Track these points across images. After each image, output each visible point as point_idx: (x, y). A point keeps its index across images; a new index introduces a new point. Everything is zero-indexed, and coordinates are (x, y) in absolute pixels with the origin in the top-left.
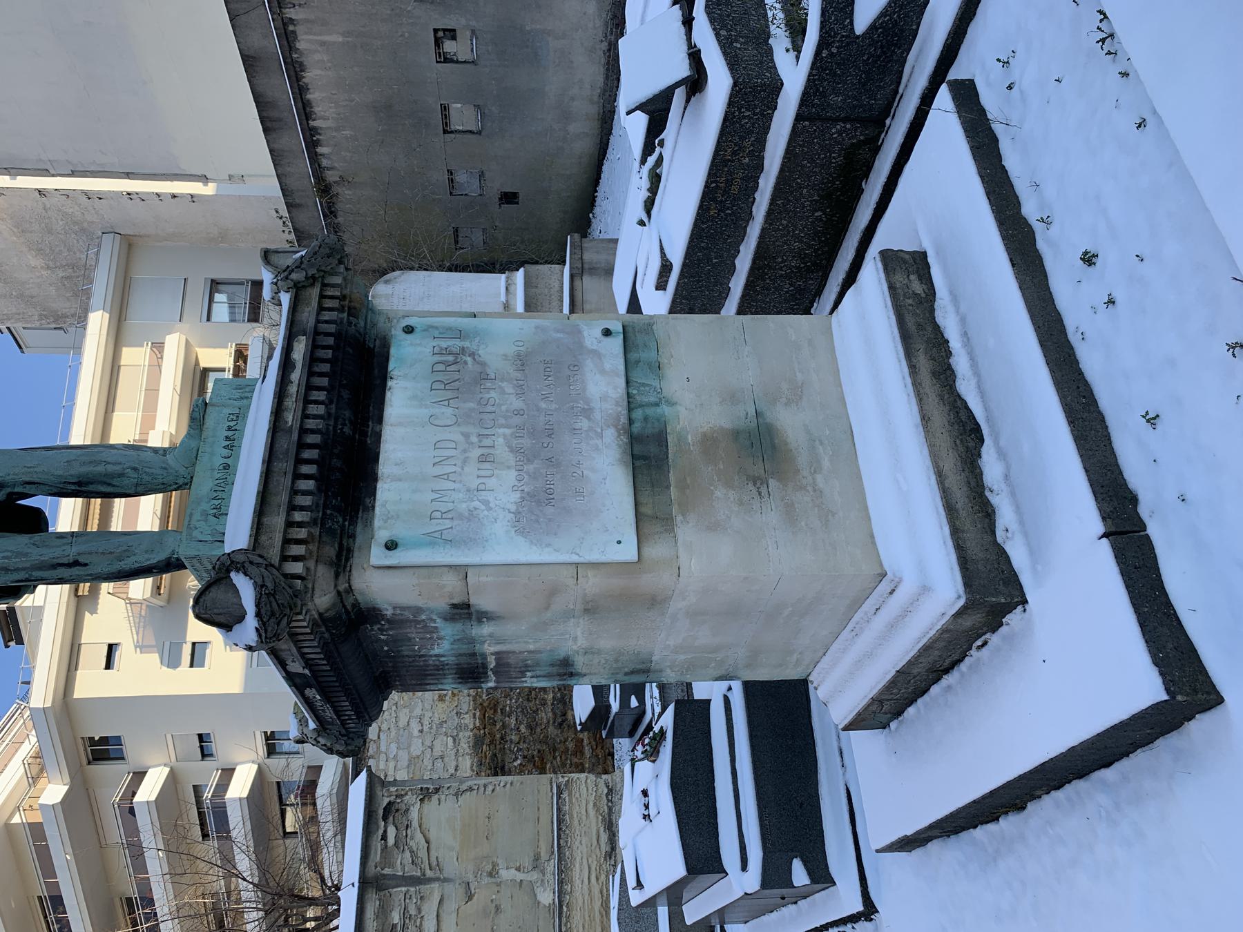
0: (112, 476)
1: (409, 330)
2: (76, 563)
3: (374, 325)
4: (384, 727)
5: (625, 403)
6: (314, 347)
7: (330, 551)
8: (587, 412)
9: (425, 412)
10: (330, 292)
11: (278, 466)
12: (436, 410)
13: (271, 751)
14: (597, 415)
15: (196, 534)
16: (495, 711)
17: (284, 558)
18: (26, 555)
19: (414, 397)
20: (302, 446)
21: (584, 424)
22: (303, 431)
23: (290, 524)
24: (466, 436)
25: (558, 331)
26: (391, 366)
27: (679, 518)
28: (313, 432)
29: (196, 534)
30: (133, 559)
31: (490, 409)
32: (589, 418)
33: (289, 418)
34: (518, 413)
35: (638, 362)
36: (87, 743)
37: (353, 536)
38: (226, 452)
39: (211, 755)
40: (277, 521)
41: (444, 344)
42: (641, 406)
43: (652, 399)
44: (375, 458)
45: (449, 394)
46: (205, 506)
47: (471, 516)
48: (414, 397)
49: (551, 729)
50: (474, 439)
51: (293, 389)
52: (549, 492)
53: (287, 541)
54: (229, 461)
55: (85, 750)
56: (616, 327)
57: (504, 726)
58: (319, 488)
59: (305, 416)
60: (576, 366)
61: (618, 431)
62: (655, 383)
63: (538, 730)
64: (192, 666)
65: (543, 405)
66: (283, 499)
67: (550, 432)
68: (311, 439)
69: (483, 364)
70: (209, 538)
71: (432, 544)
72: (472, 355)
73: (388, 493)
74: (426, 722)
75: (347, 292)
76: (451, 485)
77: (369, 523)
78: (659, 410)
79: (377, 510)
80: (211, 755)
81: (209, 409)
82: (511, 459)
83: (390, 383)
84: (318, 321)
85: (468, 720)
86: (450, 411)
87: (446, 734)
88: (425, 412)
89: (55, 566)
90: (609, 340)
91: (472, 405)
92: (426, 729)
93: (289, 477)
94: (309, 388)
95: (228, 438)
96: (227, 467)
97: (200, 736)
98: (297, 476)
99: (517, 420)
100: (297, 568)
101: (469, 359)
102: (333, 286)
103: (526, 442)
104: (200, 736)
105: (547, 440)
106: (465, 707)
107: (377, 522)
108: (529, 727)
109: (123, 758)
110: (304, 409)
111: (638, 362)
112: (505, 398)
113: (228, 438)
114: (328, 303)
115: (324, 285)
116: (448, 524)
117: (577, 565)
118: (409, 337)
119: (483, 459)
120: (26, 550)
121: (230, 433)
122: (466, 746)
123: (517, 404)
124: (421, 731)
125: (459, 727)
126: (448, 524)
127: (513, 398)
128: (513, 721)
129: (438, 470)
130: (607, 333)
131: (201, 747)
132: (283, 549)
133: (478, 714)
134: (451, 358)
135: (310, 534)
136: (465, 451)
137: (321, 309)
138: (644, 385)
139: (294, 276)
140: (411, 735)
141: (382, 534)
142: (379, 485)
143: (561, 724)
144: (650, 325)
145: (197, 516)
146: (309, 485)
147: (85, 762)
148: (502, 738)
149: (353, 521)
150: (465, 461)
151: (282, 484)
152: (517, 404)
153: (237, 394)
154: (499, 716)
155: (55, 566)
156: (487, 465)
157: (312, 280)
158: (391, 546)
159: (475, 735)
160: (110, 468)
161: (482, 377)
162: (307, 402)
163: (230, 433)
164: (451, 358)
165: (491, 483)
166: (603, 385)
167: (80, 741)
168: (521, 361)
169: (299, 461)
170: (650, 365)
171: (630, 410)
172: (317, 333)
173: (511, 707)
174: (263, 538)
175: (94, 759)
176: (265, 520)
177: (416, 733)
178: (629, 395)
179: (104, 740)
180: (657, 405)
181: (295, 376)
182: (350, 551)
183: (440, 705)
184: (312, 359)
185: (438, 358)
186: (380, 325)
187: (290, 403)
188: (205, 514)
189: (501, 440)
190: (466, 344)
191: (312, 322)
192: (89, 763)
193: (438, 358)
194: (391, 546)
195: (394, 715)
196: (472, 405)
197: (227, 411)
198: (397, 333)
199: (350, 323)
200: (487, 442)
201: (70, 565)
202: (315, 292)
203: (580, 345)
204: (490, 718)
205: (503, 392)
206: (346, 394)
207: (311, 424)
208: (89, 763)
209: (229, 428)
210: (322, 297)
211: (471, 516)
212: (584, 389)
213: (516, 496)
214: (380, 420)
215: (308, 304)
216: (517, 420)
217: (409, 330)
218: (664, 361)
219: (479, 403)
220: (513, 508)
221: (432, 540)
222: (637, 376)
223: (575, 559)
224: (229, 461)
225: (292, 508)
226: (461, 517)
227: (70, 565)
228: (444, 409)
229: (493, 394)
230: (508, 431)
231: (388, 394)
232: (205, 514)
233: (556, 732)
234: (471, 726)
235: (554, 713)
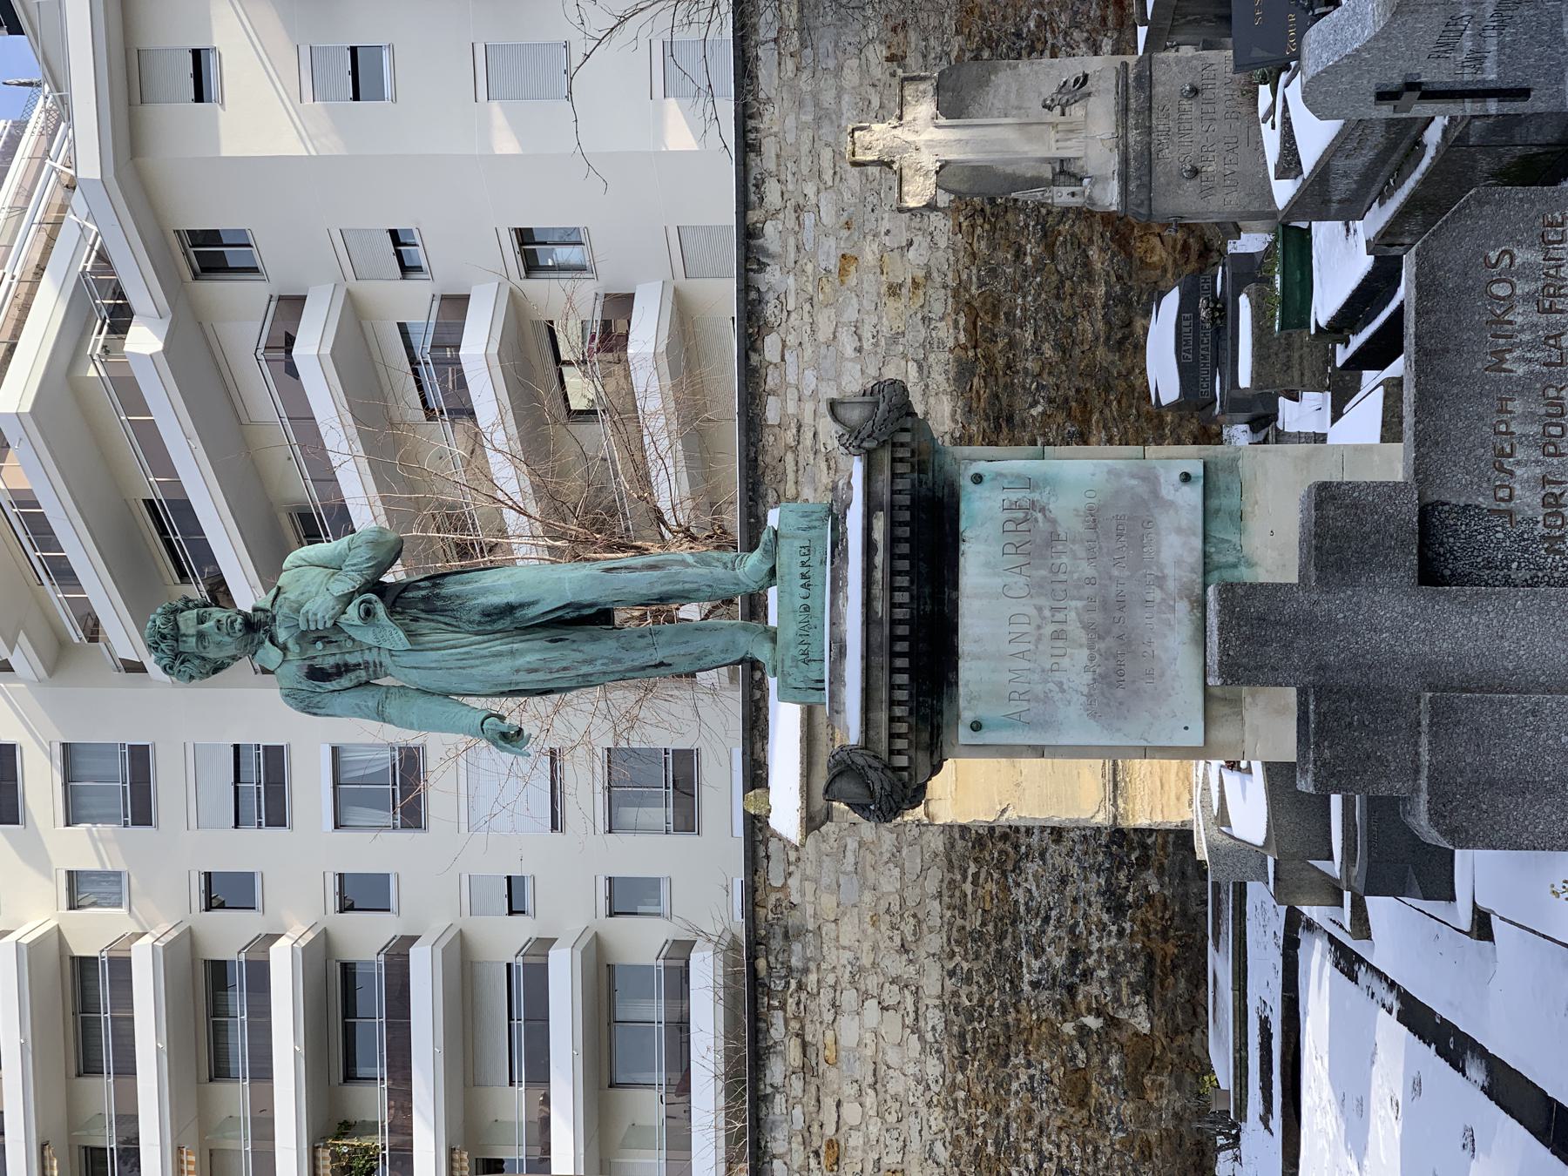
0: (689, 591)
1: (978, 479)
2: (661, 664)
3: (941, 468)
4: (792, 340)
5: (1201, 570)
6: (893, 524)
7: (925, 737)
8: (1160, 581)
9: (999, 582)
10: (903, 453)
11: (875, 660)
12: (1010, 579)
13: (531, 266)
14: (1171, 585)
15: (790, 680)
16: (995, 316)
17: (892, 752)
18: (619, 661)
19: (987, 564)
20: (894, 638)
21: (1157, 595)
22: (894, 622)
23: (892, 719)
24: (1040, 609)
25: (1133, 476)
26: (963, 525)
27: (1248, 700)
28: (901, 622)
29: (790, 680)
30: (710, 658)
31: (1062, 577)
32: (1161, 587)
33: (880, 607)
34: (1090, 581)
35: (1218, 511)
36: (187, 240)
37: (941, 713)
38: (803, 592)
39: (419, 269)
40: (882, 716)
41: (1014, 496)
42: (1218, 568)
43: (1231, 559)
44: (953, 629)
45: (1021, 560)
46: (794, 651)
47: (1047, 699)
48: (987, 564)
49: (1101, 352)
50: (1047, 613)
51: (878, 575)
52: (1119, 673)
53: (892, 736)
54: (808, 602)
55: (186, 253)
56: (1196, 469)
57: (1012, 344)
58: (911, 679)
59: (893, 605)
60: (1148, 523)
61: (1191, 603)
62: (1235, 539)
63: (1077, 351)
64: (356, 97)
65: (1116, 573)
66: (884, 695)
67: (1121, 604)
68: (903, 630)
69: (1053, 522)
70: (802, 685)
71: (1012, 726)
72: (1043, 510)
73: (970, 672)
74: (867, 333)
75: (915, 445)
76: (1027, 665)
77: (954, 699)
78: (1236, 573)
79: (962, 690)
80: (419, 269)
81: (781, 541)
82: (1081, 635)
83: (963, 547)
84: (893, 492)
85: (944, 332)
86: (1022, 580)
87: (904, 356)
88: (999, 582)
89: (643, 668)
90: (1186, 489)
91: (1043, 573)
92: (867, 346)
93: (886, 672)
94: (894, 573)
95: (803, 576)
96: (807, 609)
97: (394, 234)
98: (893, 671)
99: (1088, 591)
100: (902, 761)
101: (1039, 515)
102: (902, 445)
103: (1097, 617)
104: (394, 234)
105: (1118, 614)
106: (938, 309)
107: (962, 703)
108: (1058, 346)
109: (255, 270)
110: (892, 598)
111: (1218, 511)
112: (1076, 565)
113: (803, 576)
114: (902, 468)
115: (894, 445)
116: (1025, 706)
117: (1145, 748)
118: (978, 488)
119: (1057, 636)
120: (619, 656)
121: (804, 570)
122: (941, 379)
123: (1087, 570)
124: (859, 350)
125: (927, 345)
126: (1025, 706)
127: (1084, 564)
128: (1029, 335)
129: (1014, 648)
130: (1186, 478)
131: (399, 254)
132: (890, 744)
133: (962, 321)
134: (1020, 515)
135: (910, 728)
136: (1039, 627)
137: (894, 475)
138: (1224, 541)
139: (865, 444)
140: (841, 357)
141: (967, 716)
142: (961, 663)
143: (1120, 342)
144: (1235, 460)
145: (788, 663)
146: (903, 679)
147: (188, 275)
148: (1008, 366)
149: (940, 700)
150: (1039, 639)
151: (882, 679)
152: (1087, 570)
153: (804, 523)
154: (1001, 326)
155: (643, 668)
156: (1060, 643)
157: (883, 444)
158: (976, 726)
159: (958, 360)
160: (687, 586)
161: (1053, 538)
162: (893, 589)
163: (804, 570)
164: (1020, 515)
165: (1065, 662)
166: (1176, 548)
167: (174, 238)
168: (1093, 517)
169: (893, 655)
170: (1231, 514)
171: (1205, 573)
172: (892, 506)
173: (1024, 310)
174: (872, 733)
175: (205, 270)
176: (872, 715)
177: (849, 352)
178: (1205, 555)
179: (212, 237)
180: (1235, 566)
181: (879, 559)
182: (939, 727)
183: (891, 302)
184: (893, 540)
185: (1008, 515)
186: (947, 467)
187: (877, 590)
188: (794, 659)
189: (1073, 615)
190: (1036, 496)
191: (886, 497)
192: (196, 277)
193: (1008, 515)
194: (976, 726)
195: (806, 316)
196: (1043, 573)
197: (798, 543)
198: (965, 482)
199: (920, 482)
200: (1060, 616)
201: (656, 666)
202: (885, 456)
203: (1155, 493)
204: (985, 329)
205: (1075, 558)
206: (923, 567)
207: (900, 613)
208: (196, 277)
209: (803, 564)
210: (894, 460)
211: (1047, 699)
212: (1158, 552)
213: (1088, 677)
214: (955, 585)
215: (881, 472)
216: (1088, 591)
217: (978, 479)
218: (1247, 509)
219: (1051, 571)
220: (1086, 691)
221: (1012, 722)
222: (1217, 531)
223: (1145, 744)
224: (808, 602)
225: (892, 703)
226: (1037, 699)
227: (656, 666)
228: (1017, 578)
229: (1064, 559)
230: (1080, 604)
231: (962, 560)
232: (794, 659)
233: (1111, 357)
234: (951, 343)
235: (1108, 323)
